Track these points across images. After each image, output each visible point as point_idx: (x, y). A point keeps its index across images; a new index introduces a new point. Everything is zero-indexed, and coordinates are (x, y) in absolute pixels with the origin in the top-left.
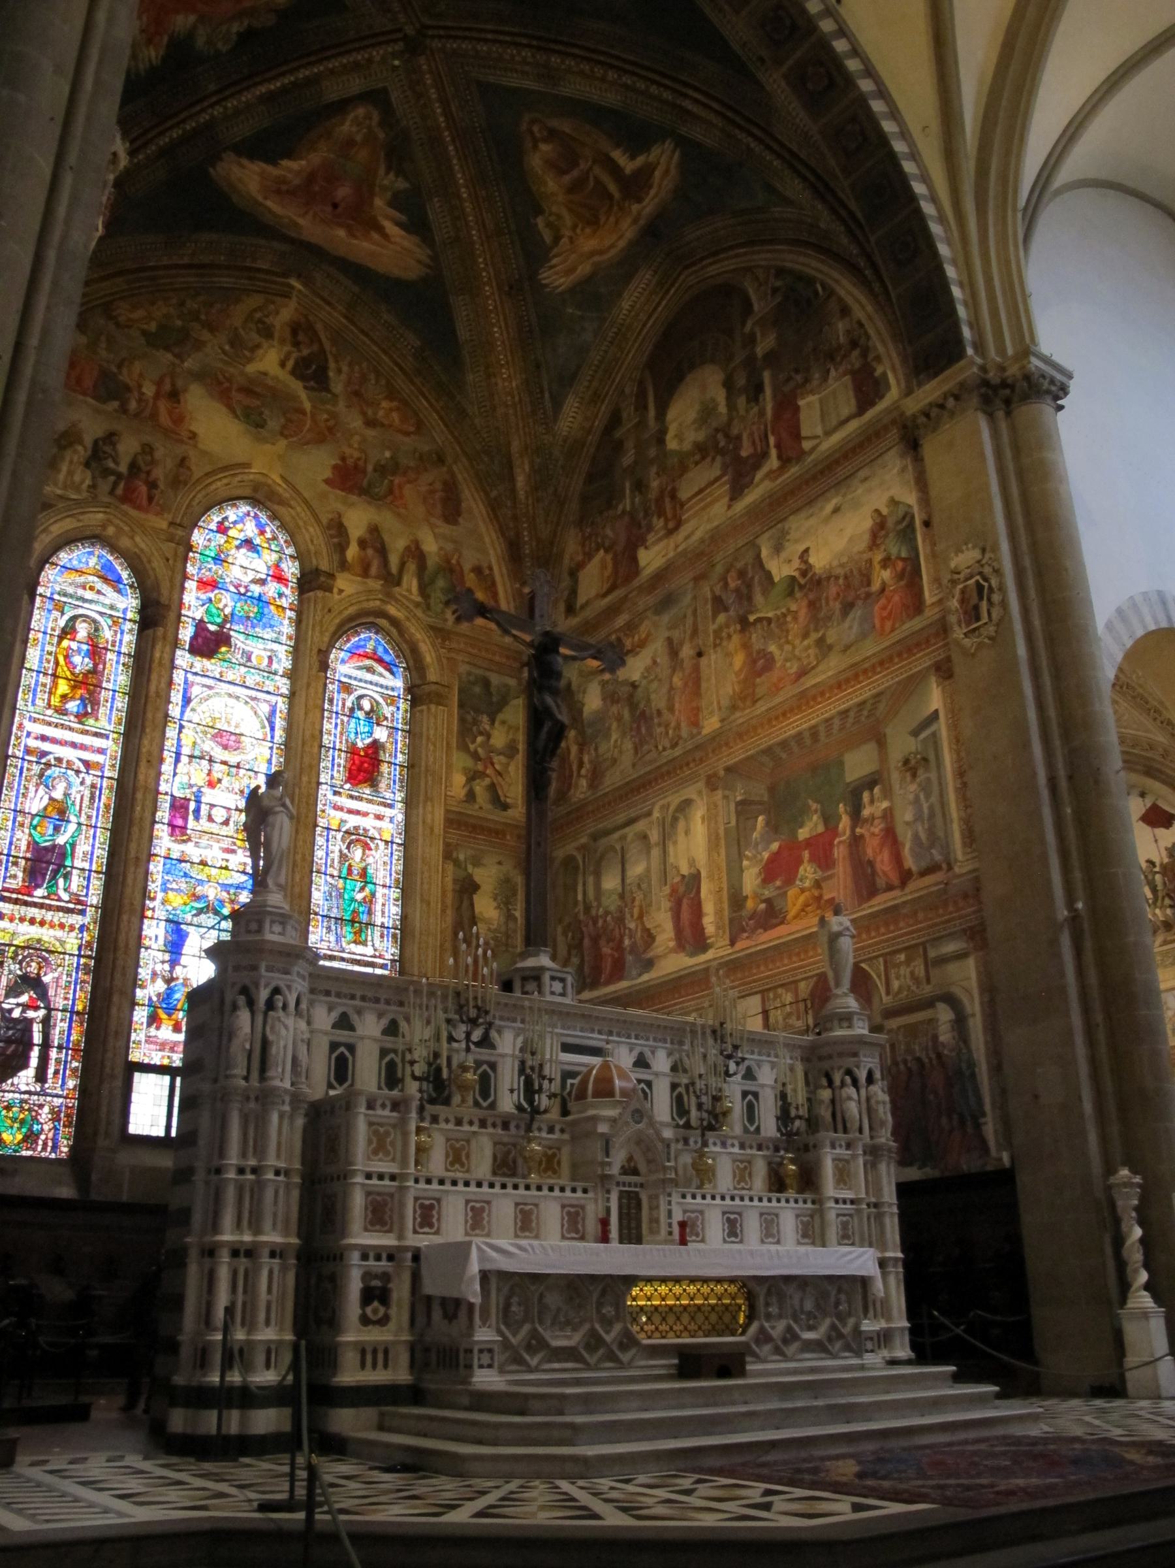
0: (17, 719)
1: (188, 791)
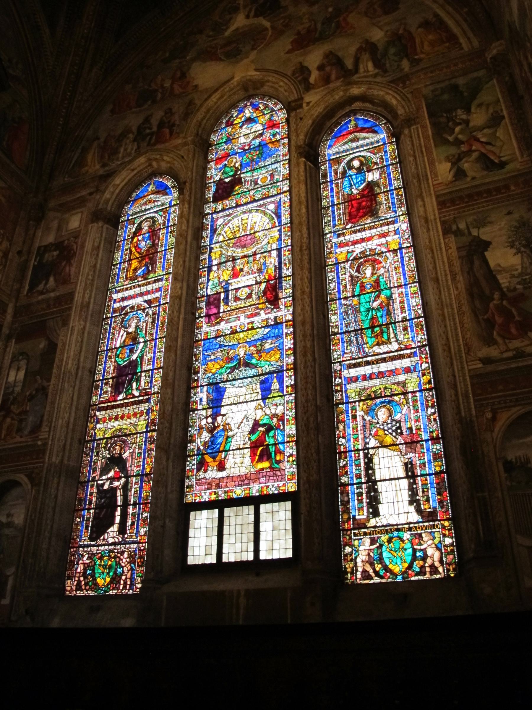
0: (109, 295)
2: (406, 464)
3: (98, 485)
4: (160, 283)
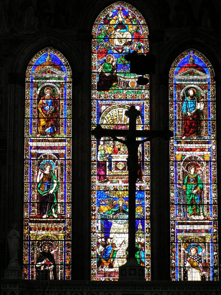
1: (105, 157)
2: (202, 277)
4: (64, 143)
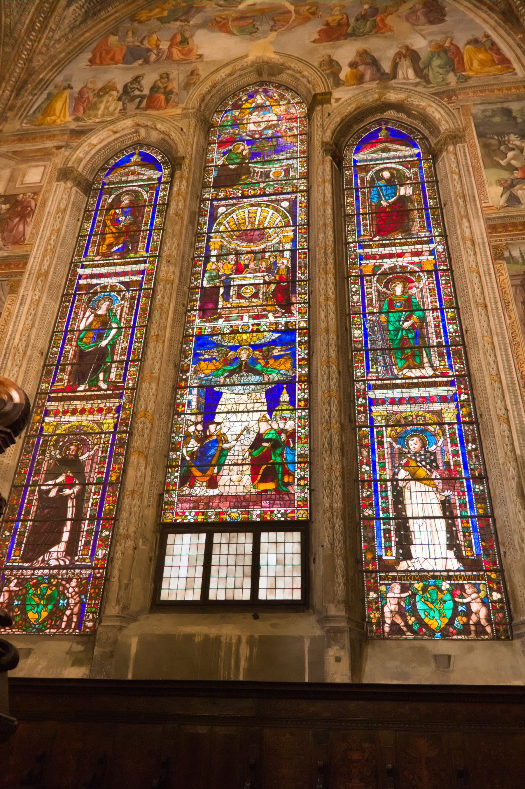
2: (443, 503)
3: (40, 491)
4: (143, 265)
